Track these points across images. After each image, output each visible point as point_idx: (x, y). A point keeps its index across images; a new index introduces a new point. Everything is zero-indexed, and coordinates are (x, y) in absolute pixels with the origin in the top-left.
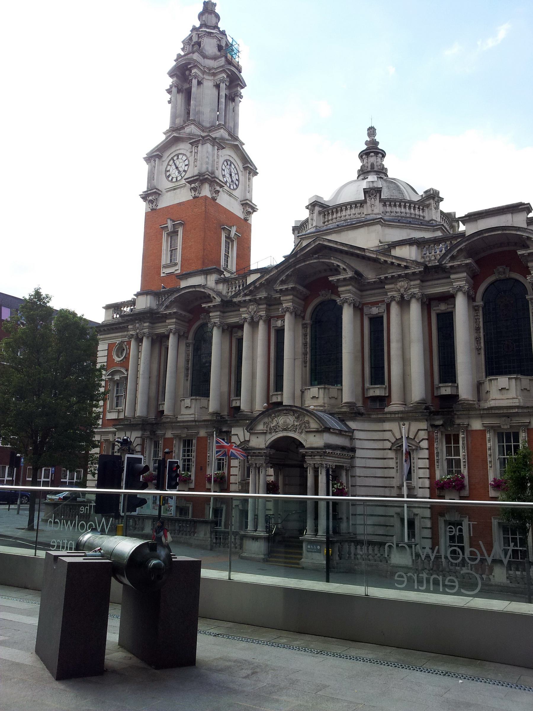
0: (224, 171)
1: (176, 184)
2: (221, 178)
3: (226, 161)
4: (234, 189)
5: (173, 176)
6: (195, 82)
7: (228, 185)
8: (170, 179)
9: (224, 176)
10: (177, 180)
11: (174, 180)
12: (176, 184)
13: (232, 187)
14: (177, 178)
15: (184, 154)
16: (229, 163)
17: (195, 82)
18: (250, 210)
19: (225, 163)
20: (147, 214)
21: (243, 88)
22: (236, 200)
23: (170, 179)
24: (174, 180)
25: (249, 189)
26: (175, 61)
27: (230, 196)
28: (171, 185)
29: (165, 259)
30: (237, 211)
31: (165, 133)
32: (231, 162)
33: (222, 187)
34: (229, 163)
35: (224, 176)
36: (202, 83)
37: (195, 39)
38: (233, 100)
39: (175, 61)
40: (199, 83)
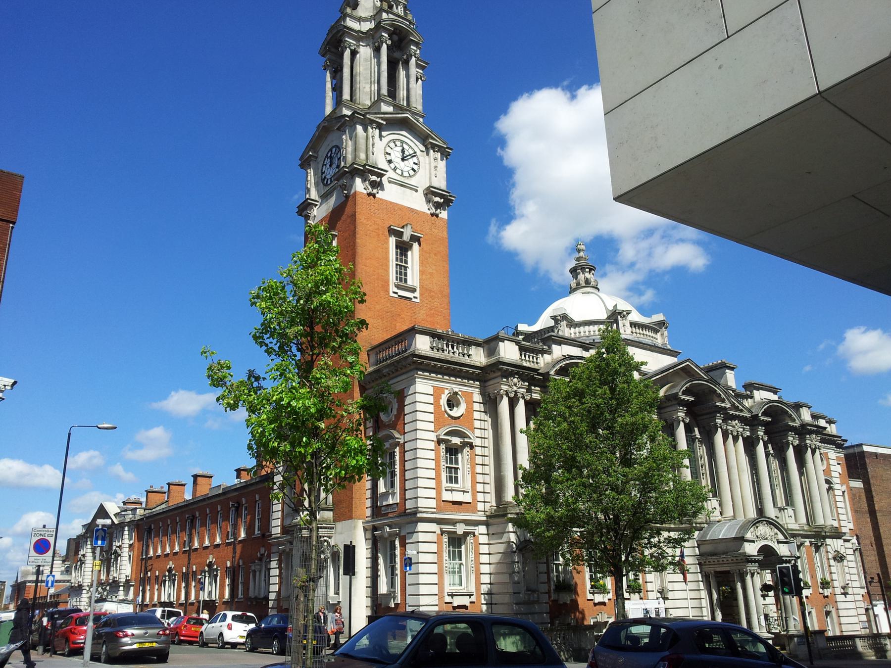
3: (394, 141)
4: (410, 176)
9: (390, 162)
13: (406, 174)
16: (398, 143)
17: (347, 54)
19: (392, 145)
22: (416, 191)
32: (402, 142)
34: (398, 143)
36: (358, 52)
40: (354, 53)
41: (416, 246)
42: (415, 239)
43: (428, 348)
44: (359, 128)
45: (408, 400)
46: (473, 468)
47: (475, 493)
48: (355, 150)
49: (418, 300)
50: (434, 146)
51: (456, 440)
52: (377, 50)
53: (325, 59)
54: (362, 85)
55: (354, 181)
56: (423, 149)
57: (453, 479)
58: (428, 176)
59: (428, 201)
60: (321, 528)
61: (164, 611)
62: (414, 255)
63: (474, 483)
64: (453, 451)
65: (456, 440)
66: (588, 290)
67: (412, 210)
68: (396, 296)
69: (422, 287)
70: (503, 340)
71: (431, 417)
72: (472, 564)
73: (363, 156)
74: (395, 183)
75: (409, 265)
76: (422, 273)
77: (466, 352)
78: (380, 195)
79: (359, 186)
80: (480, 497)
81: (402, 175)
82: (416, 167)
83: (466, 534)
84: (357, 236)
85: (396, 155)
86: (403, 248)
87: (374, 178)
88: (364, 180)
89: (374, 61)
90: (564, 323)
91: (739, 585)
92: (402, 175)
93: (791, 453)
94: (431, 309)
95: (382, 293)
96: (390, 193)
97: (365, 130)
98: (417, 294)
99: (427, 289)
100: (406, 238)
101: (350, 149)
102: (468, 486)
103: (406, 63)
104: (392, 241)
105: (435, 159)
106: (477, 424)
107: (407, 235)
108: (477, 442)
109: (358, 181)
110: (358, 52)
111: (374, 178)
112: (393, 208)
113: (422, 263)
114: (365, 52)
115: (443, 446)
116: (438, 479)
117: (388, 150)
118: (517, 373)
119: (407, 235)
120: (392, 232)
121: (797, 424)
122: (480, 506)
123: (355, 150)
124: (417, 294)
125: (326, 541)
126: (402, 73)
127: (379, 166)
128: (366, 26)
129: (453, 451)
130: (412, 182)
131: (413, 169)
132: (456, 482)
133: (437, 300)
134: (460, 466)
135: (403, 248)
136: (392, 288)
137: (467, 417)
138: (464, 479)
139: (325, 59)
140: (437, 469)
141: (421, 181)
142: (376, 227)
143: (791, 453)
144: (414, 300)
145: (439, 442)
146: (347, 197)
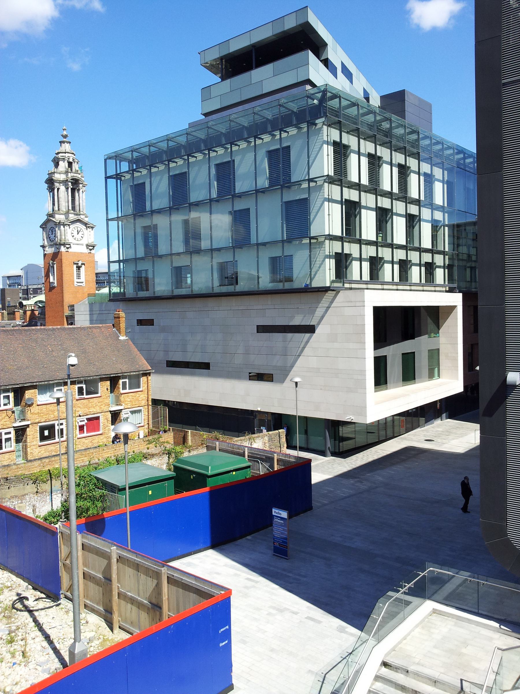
17: (56, 190)
19: (74, 229)
40: (58, 189)
42: (82, 264)
44: (62, 227)
50: (89, 227)
52: (67, 189)
54: (62, 203)
56: (85, 227)
59: (87, 248)
62: (83, 269)
67: (82, 253)
69: (86, 280)
73: (63, 237)
78: (70, 250)
82: (82, 236)
85: (75, 232)
86: (79, 268)
87: (68, 246)
88: (64, 247)
89: (66, 193)
96: (74, 249)
97: (64, 227)
98: (84, 283)
100: (80, 265)
101: (59, 234)
103: (79, 190)
104: (75, 266)
109: (62, 247)
112: (75, 254)
113: (86, 272)
114: (62, 188)
120: (74, 264)
124: (84, 283)
126: (77, 194)
128: (62, 177)
135: (79, 268)
136: (75, 283)
141: (85, 242)
146: (59, 251)
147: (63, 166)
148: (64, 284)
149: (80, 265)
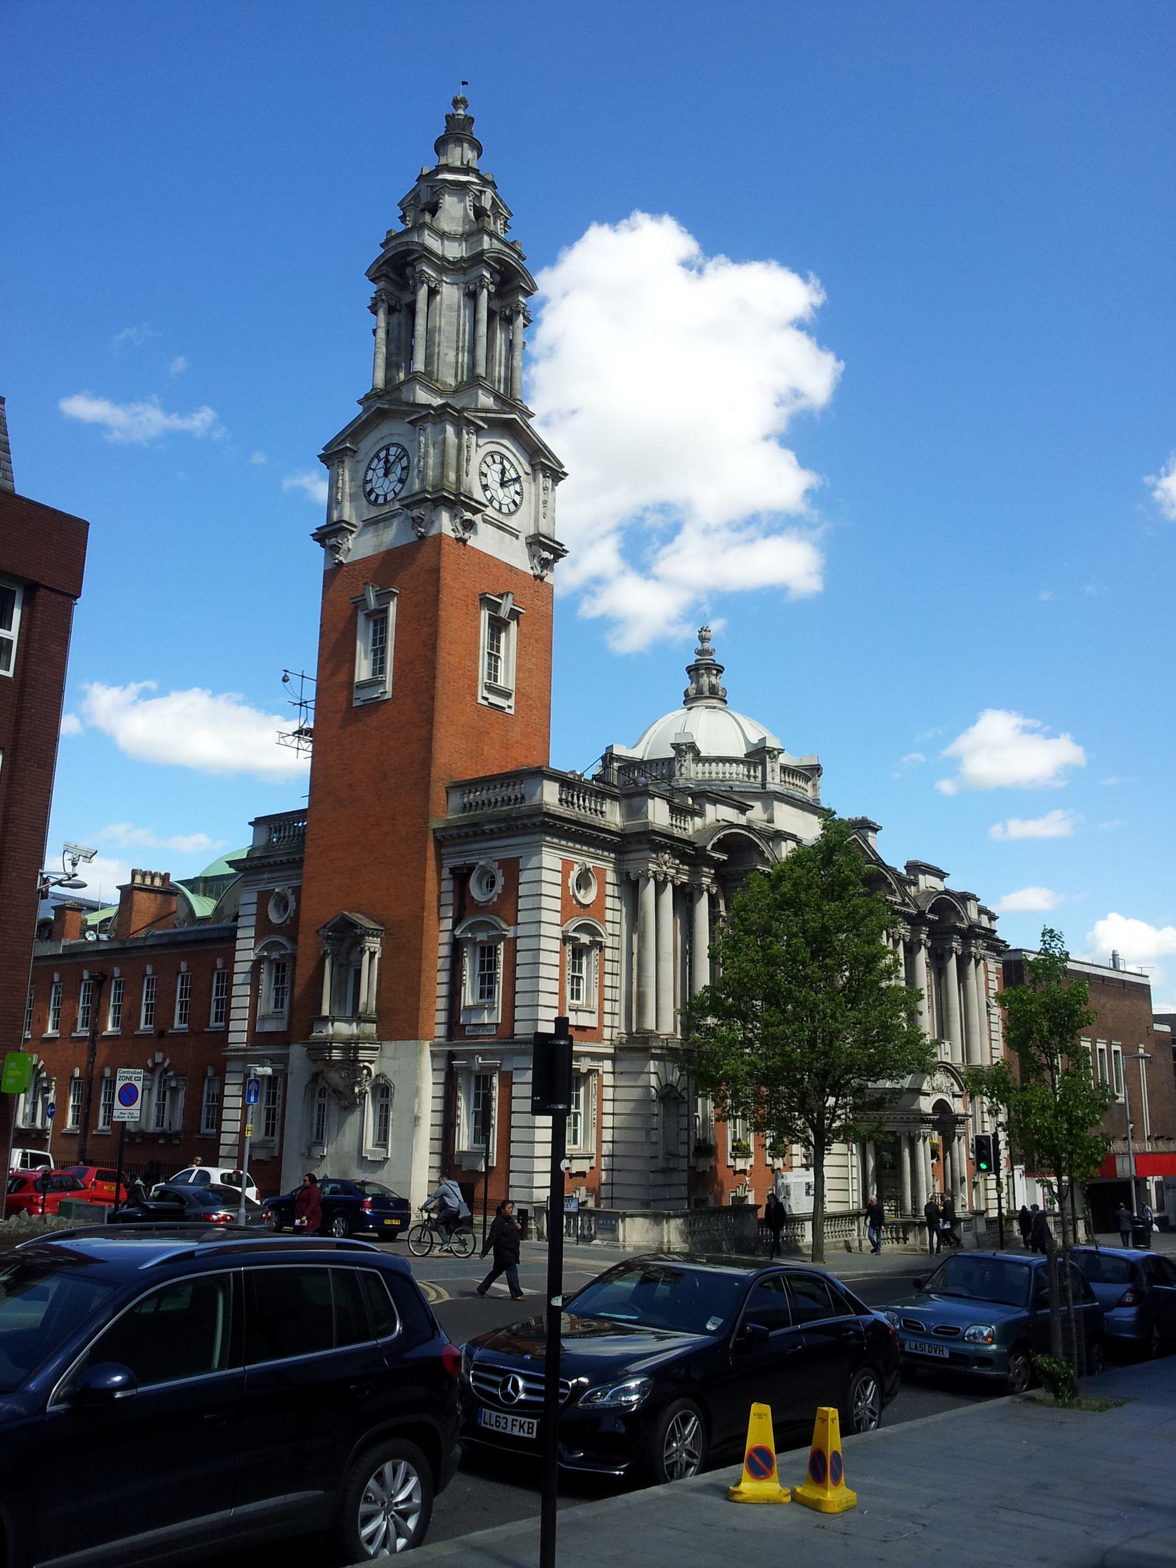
0: (486, 476)
1: (386, 509)
2: (478, 494)
3: (492, 454)
4: (511, 513)
5: (379, 491)
6: (423, 292)
7: (496, 505)
8: (373, 497)
9: (485, 487)
10: (385, 499)
11: (381, 500)
12: (386, 509)
13: (505, 509)
14: (385, 496)
15: (398, 445)
16: (497, 458)
17: (423, 292)
18: (546, 555)
19: (489, 460)
20: (326, 573)
21: (528, 294)
22: (517, 537)
23: (373, 497)
24: (381, 500)
25: (545, 506)
26: (382, 245)
27: (499, 528)
28: (374, 512)
29: (363, 670)
30: (517, 556)
31: (360, 402)
32: (503, 457)
33: (476, 511)
34: (497, 458)
35: (485, 487)
36: (438, 292)
37: (425, 197)
38: (509, 321)
39: (382, 245)
40: (433, 293)
41: (513, 626)
43: (557, 802)
44: (450, 430)
45: (524, 877)
46: (601, 978)
47: (602, 1013)
48: (443, 464)
49: (512, 711)
51: (585, 939)
53: (374, 287)
54: (444, 349)
55: (439, 517)
56: (529, 470)
57: (576, 994)
58: (533, 515)
59: (533, 556)
60: (363, 1049)
61: (24, 1155)
62: (510, 640)
63: (602, 999)
64: (579, 952)
65: (585, 939)
66: (715, 702)
68: (485, 703)
70: (653, 797)
71: (558, 905)
72: (593, 1115)
73: (452, 476)
74: (492, 524)
75: (502, 654)
76: (519, 668)
77: (593, 806)
79: (446, 524)
80: (607, 1020)
81: (500, 510)
82: (517, 499)
83: (591, 1072)
84: (441, 606)
85: (493, 478)
86: (498, 626)
87: (468, 515)
88: (454, 517)
89: (465, 314)
90: (690, 756)
91: (906, 1153)
92: (500, 510)
93: (953, 964)
94: (527, 725)
95: (468, 698)
97: (459, 435)
98: (511, 702)
99: (524, 695)
100: (504, 613)
102: (595, 1003)
104: (485, 615)
105: (545, 489)
106: (609, 915)
107: (507, 605)
108: (608, 941)
109: (445, 516)
110: (438, 292)
111: (468, 515)
112: (487, 562)
114: (450, 294)
115: (569, 947)
116: (561, 994)
117: (485, 469)
118: (668, 848)
119: (507, 605)
120: (485, 601)
121: (964, 925)
122: (607, 1033)
123: (443, 464)
124: (511, 702)
125: (365, 1067)
127: (475, 497)
128: (454, 251)
129: (579, 952)
130: (513, 522)
131: (514, 502)
132: (578, 998)
133: (535, 712)
134: (584, 974)
135: (498, 626)
136: (482, 692)
137: (598, 907)
138: (588, 996)
139: (374, 287)
140: (561, 980)
142: (465, 592)
143: (953, 964)
144: (507, 710)
145: (565, 939)
147: (453, 212)
148: (440, 682)
149: (504, 613)
